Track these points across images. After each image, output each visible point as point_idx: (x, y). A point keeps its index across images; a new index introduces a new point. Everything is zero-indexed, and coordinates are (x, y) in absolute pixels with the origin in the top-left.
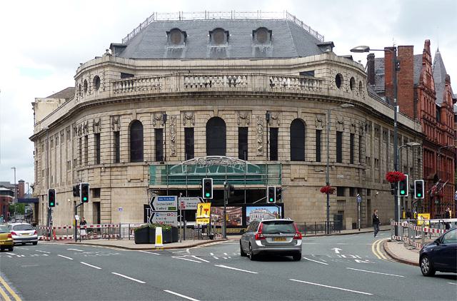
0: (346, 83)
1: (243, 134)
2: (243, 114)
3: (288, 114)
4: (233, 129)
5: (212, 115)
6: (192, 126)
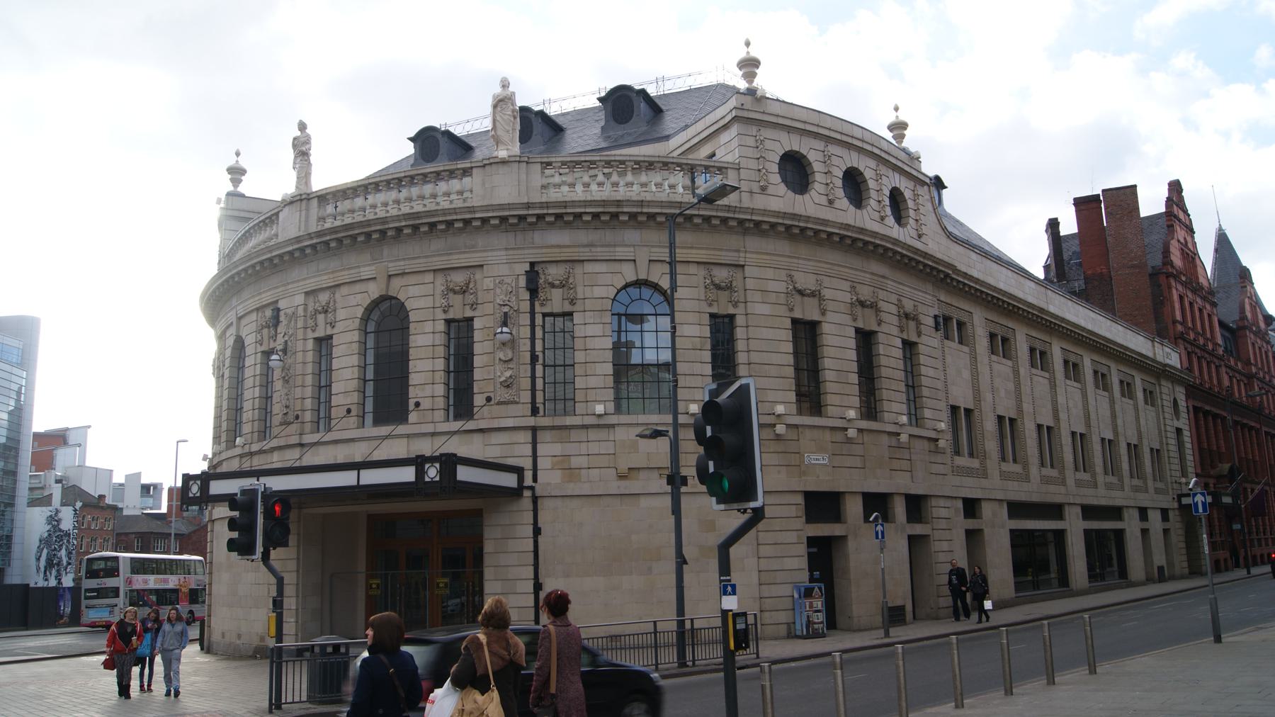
1: (460, 336)
2: (459, 278)
4: (428, 327)
5: (374, 291)
6: (329, 332)
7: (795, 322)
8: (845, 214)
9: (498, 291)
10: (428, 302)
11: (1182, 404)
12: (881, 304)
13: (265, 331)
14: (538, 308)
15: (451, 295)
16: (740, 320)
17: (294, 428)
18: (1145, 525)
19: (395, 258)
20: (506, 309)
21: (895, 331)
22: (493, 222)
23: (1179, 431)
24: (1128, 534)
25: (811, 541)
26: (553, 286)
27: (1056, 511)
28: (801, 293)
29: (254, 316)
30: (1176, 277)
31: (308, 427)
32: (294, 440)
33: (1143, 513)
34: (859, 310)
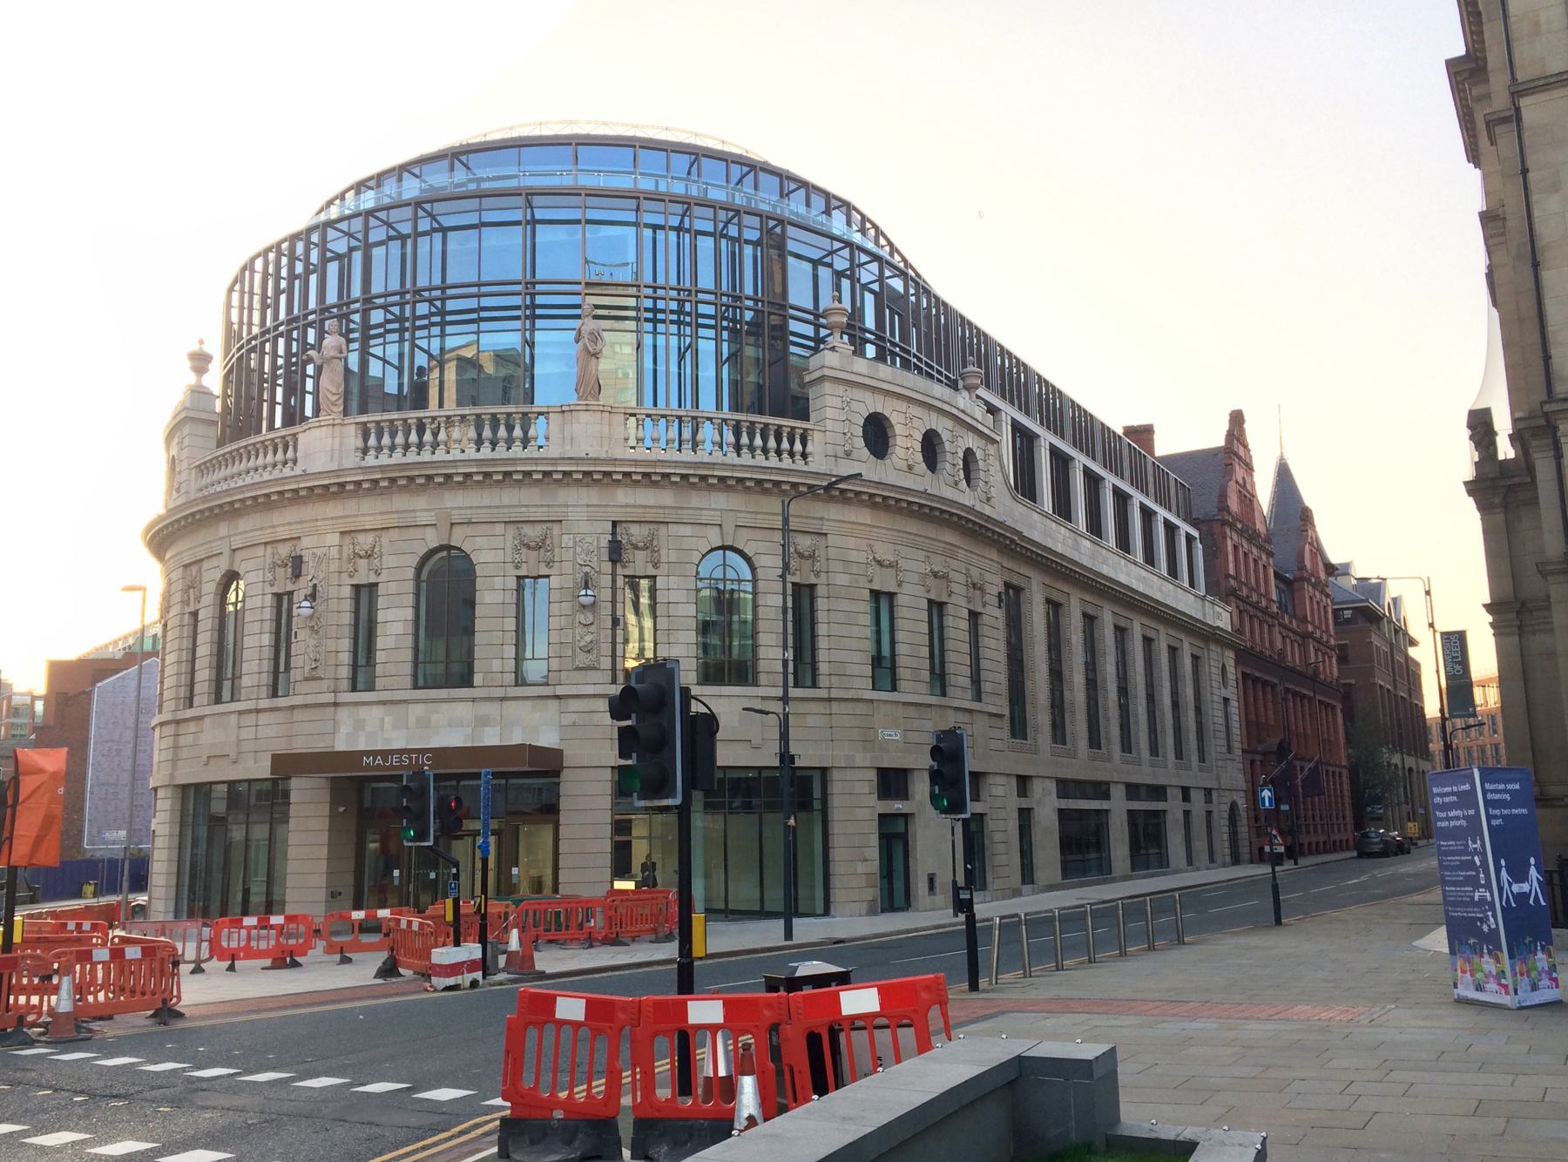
0: (906, 444)
3: (688, 530)
5: (432, 539)
6: (373, 579)
7: (872, 591)
8: (921, 481)
9: (578, 550)
10: (500, 556)
11: (1231, 670)
12: (952, 574)
13: (280, 572)
14: (619, 570)
15: (524, 550)
16: (821, 591)
17: (324, 685)
18: (1187, 806)
19: (458, 502)
20: (587, 569)
21: (963, 601)
22: (575, 476)
23: (1226, 700)
24: (1169, 817)
25: (883, 818)
26: (636, 547)
27: (1100, 790)
28: (880, 563)
29: (260, 551)
30: (1232, 526)
31: (345, 684)
32: (330, 698)
33: (1186, 793)
34: (930, 581)
